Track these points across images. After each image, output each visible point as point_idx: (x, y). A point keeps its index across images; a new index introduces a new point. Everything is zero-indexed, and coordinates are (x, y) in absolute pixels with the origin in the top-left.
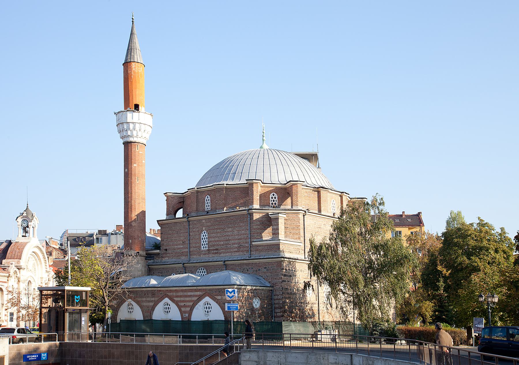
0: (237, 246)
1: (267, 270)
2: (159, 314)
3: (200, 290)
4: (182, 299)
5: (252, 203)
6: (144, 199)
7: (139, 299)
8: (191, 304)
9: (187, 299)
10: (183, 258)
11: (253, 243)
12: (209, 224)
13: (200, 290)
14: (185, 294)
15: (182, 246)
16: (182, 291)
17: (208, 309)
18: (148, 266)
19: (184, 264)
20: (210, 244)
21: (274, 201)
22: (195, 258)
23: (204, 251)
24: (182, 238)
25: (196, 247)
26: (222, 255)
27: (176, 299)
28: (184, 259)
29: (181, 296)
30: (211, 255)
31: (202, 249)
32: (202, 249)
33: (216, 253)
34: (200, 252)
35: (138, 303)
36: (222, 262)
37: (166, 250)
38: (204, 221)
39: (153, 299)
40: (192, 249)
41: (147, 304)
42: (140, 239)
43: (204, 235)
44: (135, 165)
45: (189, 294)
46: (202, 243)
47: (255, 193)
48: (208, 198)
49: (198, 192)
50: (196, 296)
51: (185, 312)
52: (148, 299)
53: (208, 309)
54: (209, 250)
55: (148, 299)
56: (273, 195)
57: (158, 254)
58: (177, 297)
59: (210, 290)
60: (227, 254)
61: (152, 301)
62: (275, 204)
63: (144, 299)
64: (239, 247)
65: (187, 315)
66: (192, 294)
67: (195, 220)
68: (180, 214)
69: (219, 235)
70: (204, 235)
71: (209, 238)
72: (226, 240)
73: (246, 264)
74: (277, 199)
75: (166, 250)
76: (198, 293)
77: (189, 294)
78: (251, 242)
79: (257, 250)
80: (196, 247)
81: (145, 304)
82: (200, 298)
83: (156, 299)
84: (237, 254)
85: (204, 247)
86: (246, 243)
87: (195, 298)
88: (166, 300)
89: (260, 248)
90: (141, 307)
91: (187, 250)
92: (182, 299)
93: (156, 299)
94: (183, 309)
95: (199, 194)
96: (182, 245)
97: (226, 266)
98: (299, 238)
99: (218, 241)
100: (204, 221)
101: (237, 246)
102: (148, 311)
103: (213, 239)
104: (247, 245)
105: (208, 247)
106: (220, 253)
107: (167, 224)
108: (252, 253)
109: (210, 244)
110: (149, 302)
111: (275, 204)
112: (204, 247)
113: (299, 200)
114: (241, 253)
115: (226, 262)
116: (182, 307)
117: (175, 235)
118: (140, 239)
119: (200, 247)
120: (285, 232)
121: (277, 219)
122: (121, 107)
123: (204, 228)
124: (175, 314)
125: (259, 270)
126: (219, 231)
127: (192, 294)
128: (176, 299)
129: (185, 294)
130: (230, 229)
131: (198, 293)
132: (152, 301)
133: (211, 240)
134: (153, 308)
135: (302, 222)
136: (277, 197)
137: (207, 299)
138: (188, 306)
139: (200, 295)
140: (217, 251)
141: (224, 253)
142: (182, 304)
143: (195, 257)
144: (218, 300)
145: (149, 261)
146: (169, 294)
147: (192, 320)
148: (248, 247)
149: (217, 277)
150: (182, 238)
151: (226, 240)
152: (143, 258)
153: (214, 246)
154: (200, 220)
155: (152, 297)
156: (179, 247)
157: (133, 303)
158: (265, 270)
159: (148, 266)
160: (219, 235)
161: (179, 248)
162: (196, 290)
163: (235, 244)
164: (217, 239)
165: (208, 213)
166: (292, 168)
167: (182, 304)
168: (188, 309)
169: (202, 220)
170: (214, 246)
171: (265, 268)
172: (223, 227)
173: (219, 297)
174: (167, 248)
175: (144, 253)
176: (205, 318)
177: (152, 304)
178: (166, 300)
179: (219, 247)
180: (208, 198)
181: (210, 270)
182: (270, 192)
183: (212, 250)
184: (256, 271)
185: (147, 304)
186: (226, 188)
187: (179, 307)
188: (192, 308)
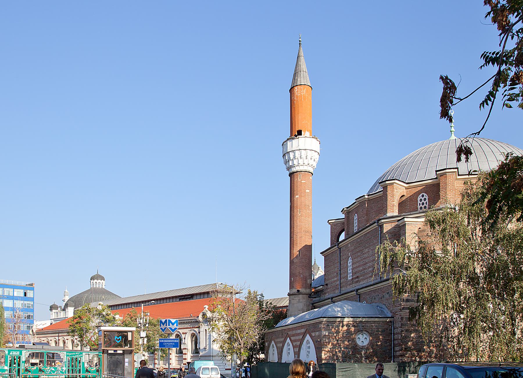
12: (353, 248)
18: (313, 304)
26: (361, 283)
33: (357, 282)
36: (355, 292)
37: (327, 285)
40: (342, 281)
42: (302, 276)
44: (297, 197)
73: (375, 291)
75: (327, 285)
95: (350, 214)
96: (337, 276)
100: (349, 245)
115: (359, 291)
118: (302, 276)
119: (347, 276)
126: (359, 254)
130: (367, 250)
145: (314, 299)
152: (305, 295)
159: (313, 304)
163: (369, 267)
164: (358, 264)
171: (388, 293)
172: (361, 248)
182: (418, 193)
186: (369, 200)
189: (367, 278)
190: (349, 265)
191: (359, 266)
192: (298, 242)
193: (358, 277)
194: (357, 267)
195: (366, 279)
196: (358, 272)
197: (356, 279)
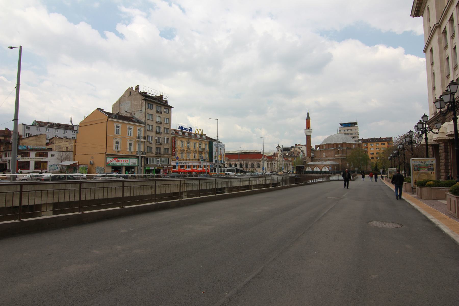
2: (315, 169)
17: (325, 168)
22: (322, 158)
28: (320, 158)
43: (324, 154)
48: (325, 146)
53: (325, 168)
68: (318, 149)
70: (324, 154)
85: (324, 156)
112: (324, 156)
124: (318, 170)
180: (325, 146)
197: (326, 156)
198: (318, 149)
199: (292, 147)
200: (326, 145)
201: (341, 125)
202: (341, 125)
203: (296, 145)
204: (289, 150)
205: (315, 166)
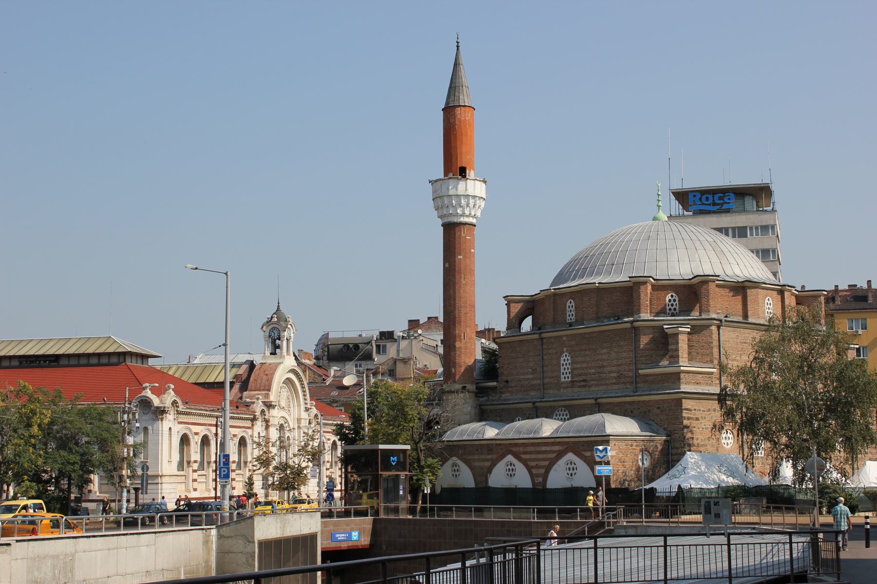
0: (615, 375)
1: (662, 411)
2: (498, 478)
3: (559, 444)
4: (533, 456)
5: (639, 312)
6: (474, 307)
7: (470, 457)
8: (547, 463)
9: (541, 456)
10: (533, 393)
11: (640, 371)
13: (559, 444)
14: (538, 449)
15: (531, 376)
16: (533, 444)
17: (572, 470)
18: (480, 406)
19: (534, 403)
20: (575, 372)
21: (672, 305)
23: (566, 383)
24: (531, 364)
25: (553, 377)
26: (593, 389)
27: (524, 456)
29: (531, 453)
30: (575, 390)
31: (563, 380)
32: (563, 380)
33: (583, 386)
34: (559, 385)
35: (468, 463)
37: (507, 382)
38: (565, 338)
39: (489, 457)
40: (546, 381)
41: (481, 464)
43: (565, 359)
45: (544, 449)
46: (562, 371)
47: (642, 295)
48: (570, 304)
49: (555, 295)
50: (554, 452)
51: (538, 475)
52: (482, 457)
54: (572, 382)
55: (482, 457)
56: (672, 296)
57: (495, 388)
58: (525, 453)
59: (574, 443)
60: (601, 388)
61: (488, 460)
62: (675, 309)
63: (476, 457)
64: (619, 377)
65: (540, 479)
66: (548, 448)
67: (551, 338)
68: (527, 325)
69: (588, 359)
70: (565, 359)
71: (572, 363)
72: (600, 367)
74: (677, 302)
76: (557, 448)
77: (544, 449)
78: (637, 369)
79: (646, 381)
80: (553, 377)
81: (477, 464)
82: (560, 455)
83: (494, 456)
84: (616, 387)
85: (565, 376)
86: (630, 370)
87: (553, 456)
88: (510, 458)
89: (650, 378)
90: (472, 468)
91: (538, 382)
92: (533, 456)
93: (494, 456)
94: (534, 471)
97: (599, 407)
98: (712, 362)
99: (586, 368)
100: (565, 338)
101: (615, 375)
102: (482, 475)
103: (579, 366)
104: (630, 374)
105: (572, 377)
106: (590, 386)
107: (509, 342)
108: (639, 385)
109: (575, 372)
110: (484, 460)
111: (675, 309)
112: (565, 376)
113: (712, 302)
114: (622, 386)
115: (599, 400)
116: (532, 467)
117: (521, 360)
119: (560, 377)
120: (689, 354)
121: (676, 335)
122: (439, 172)
123: (565, 349)
124: (522, 479)
125: (649, 411)
126: (588, 352)
127: (548, 448)
128: (522, 456)
129: (538, 449)
130: (605, 351)
131: (557, 448)
132: (488, 460)
133: (575, 366)
134: (490, 470)
135: (715, 336)
136: (677, 299)
137: (570, 456)
138: (543, 467)
139: (559, 451)
140: (585, 383)
141: (596, 385)
142: (533, 464)
143: (551, 391)
144: (586, 457)
146: (514, 449)
147: (548, 487)
148: (632, 377)
149: (584, 423)
150: (531, 364)
151: (600, 367)
153: (580, 375)
154: (558, 337)
155: (488, 454)
156: (526, 377)
157: (459, 462)
158: (658, 411)
159: (480, 406)
160: (588, 359)
161: (527, 379)
162: (553, 444)
163: (610, 372)
164: (584, 365)
165: (570, 326)
166: (701, 252)
167: (533, 464)
168: (542, 471)
169: (561, 337)
170: (580, 375)
171: (658, 408)
173: (588, 454)
174: (509, 378)
175: (471, 387)
176: (567, 484)
177: (488, 464)
178: (510, 458)
179: (588, 377)
180: (570, 304)
181: (575, 412)
183: (577, 381)
184: (645, 412)
185: (481, 464)
186: (598, 288)
187: (529, 469)
188: (548, 469)
189: (607, 384)
190: (562, 362)
191: (590, 368)
192: (463, 319)
193: (585, 381)
194: (583, 368)
195: (602, 385)
196: (586, 374)
198: (527, 325)
199: (387, 336)
200: (581, 294)
201: (682, 197)
202: (682, 197)
203: (414, 324)
204: (368, 357)
205: (497, 450)
